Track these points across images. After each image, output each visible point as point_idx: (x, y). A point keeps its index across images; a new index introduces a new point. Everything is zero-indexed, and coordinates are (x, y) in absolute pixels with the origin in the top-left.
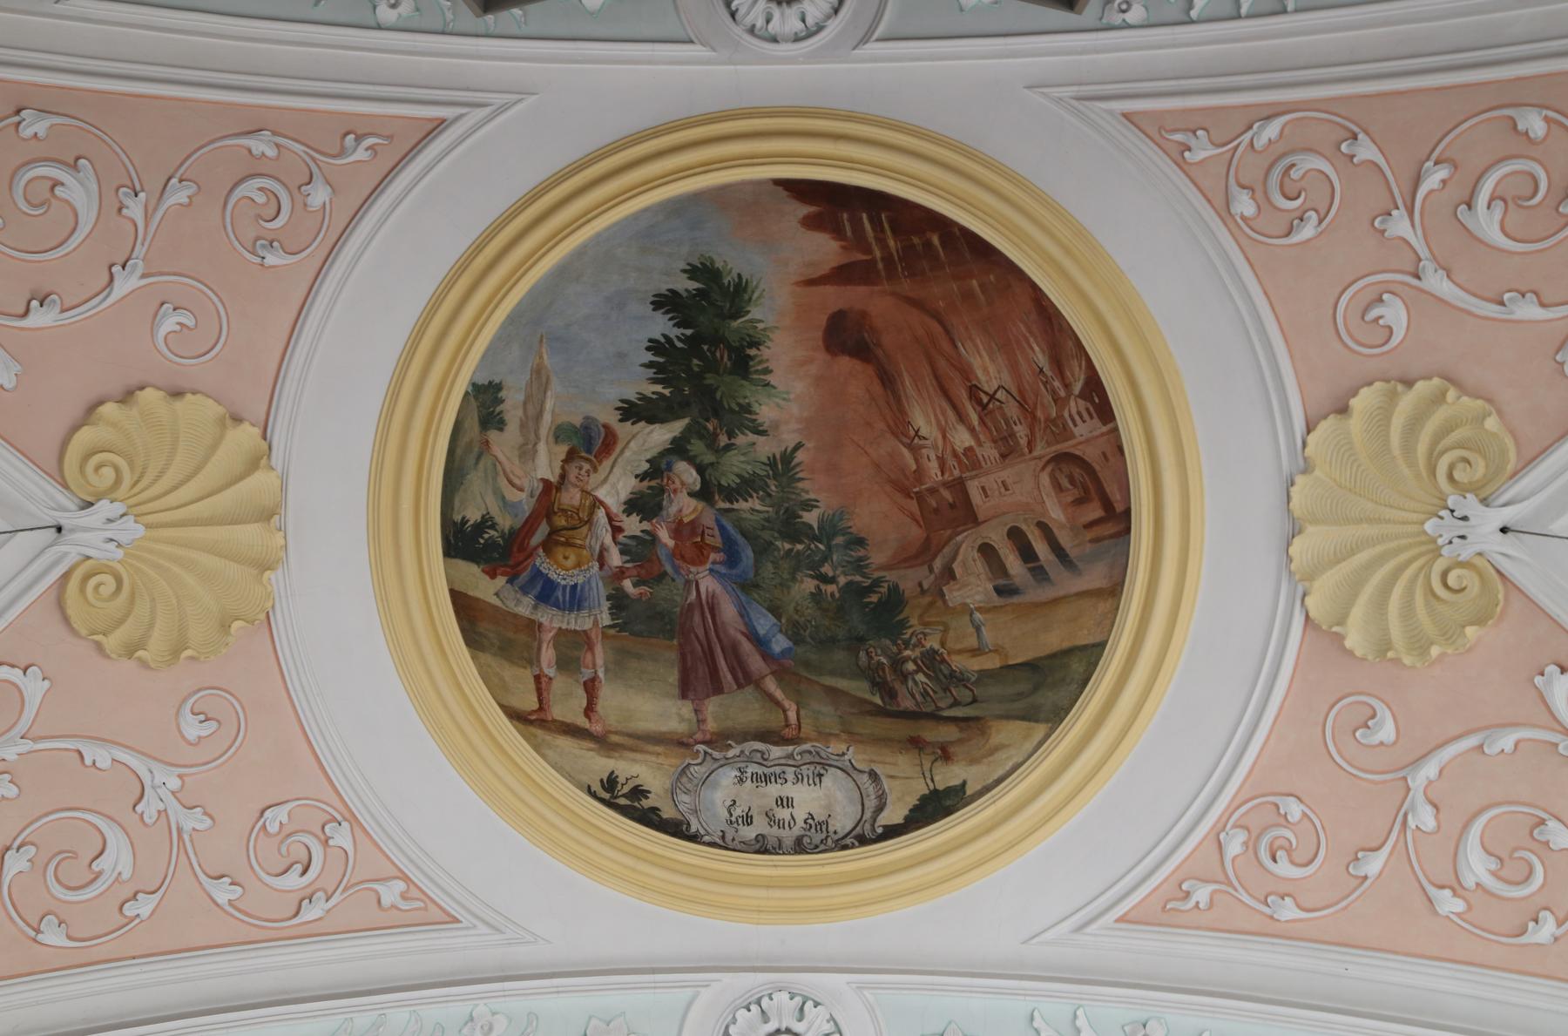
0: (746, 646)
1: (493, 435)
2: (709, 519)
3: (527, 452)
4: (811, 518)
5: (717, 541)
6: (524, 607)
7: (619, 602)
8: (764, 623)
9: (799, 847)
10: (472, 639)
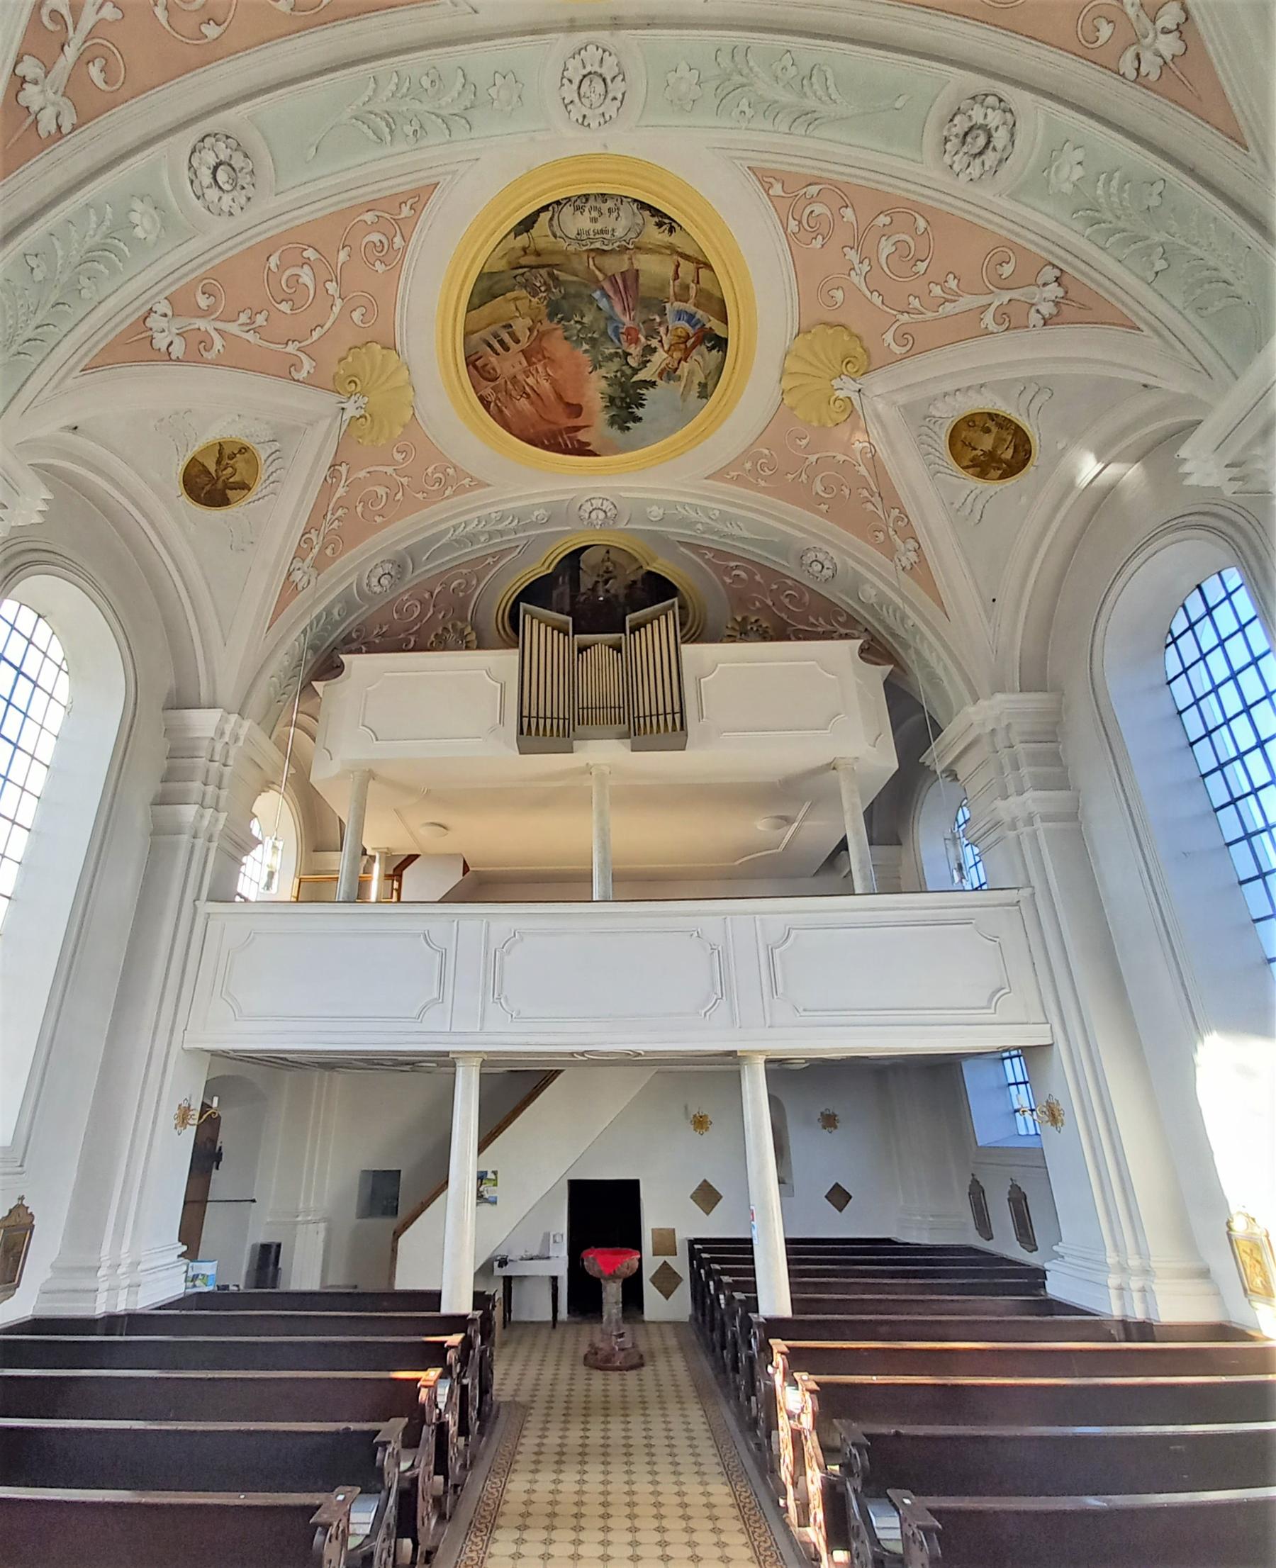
0: (611, 294)
1: (703, 381)
2: (625, 345)
3: (691, 373)
4: (585, 347)
5: (623, 337)
6: (700, 314)
7: (662, 313)
8: (604, 304)
9: (587, 197)
10: (722, 302)
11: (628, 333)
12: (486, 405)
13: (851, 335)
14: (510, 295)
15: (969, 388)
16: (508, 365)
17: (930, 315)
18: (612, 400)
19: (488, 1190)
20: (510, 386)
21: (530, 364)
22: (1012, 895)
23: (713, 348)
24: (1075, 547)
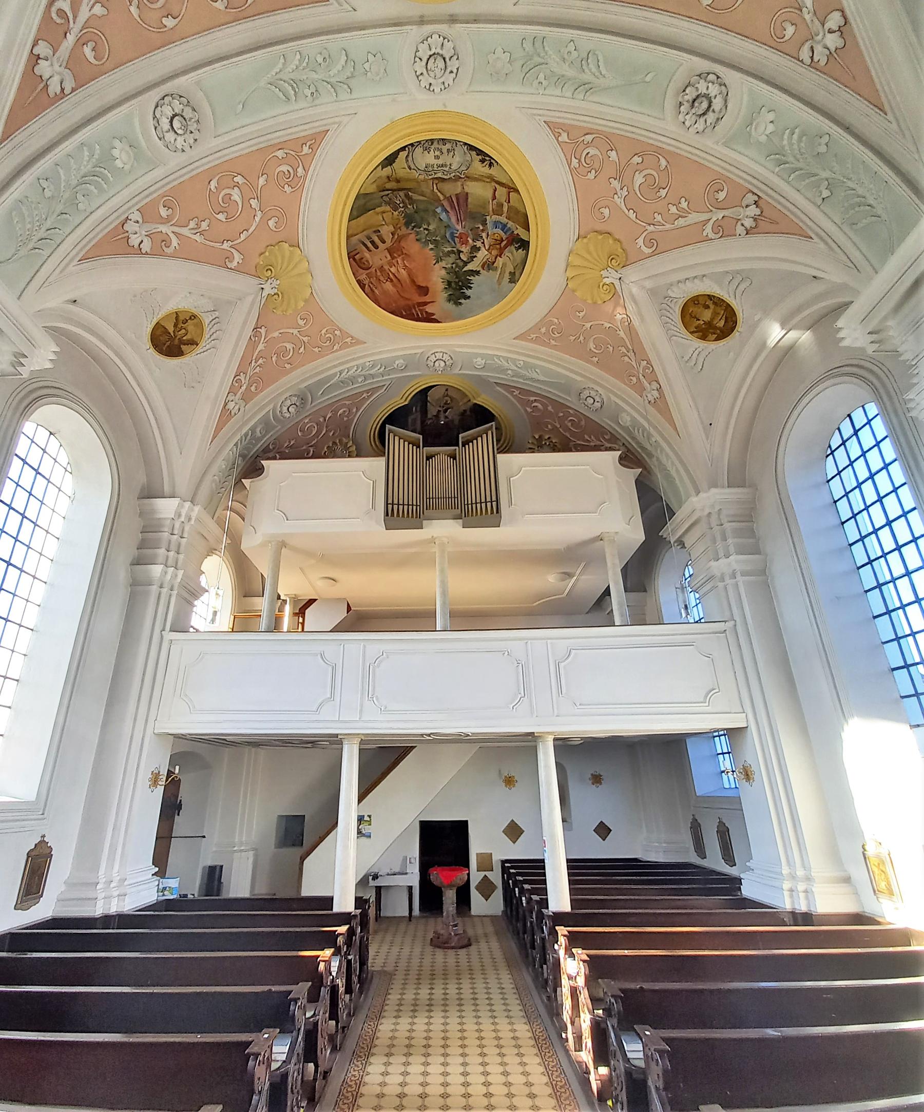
2: (458, 245)
3: (504, 265)
4: (431, 246)
6: (510, 224)
7: (484, 223)
12: (362, 287)
14: (378, 210)
16: (378, 258)
18: (449, 283)
20: (379, 274)
21: (393, 258)
23: (519, 248)
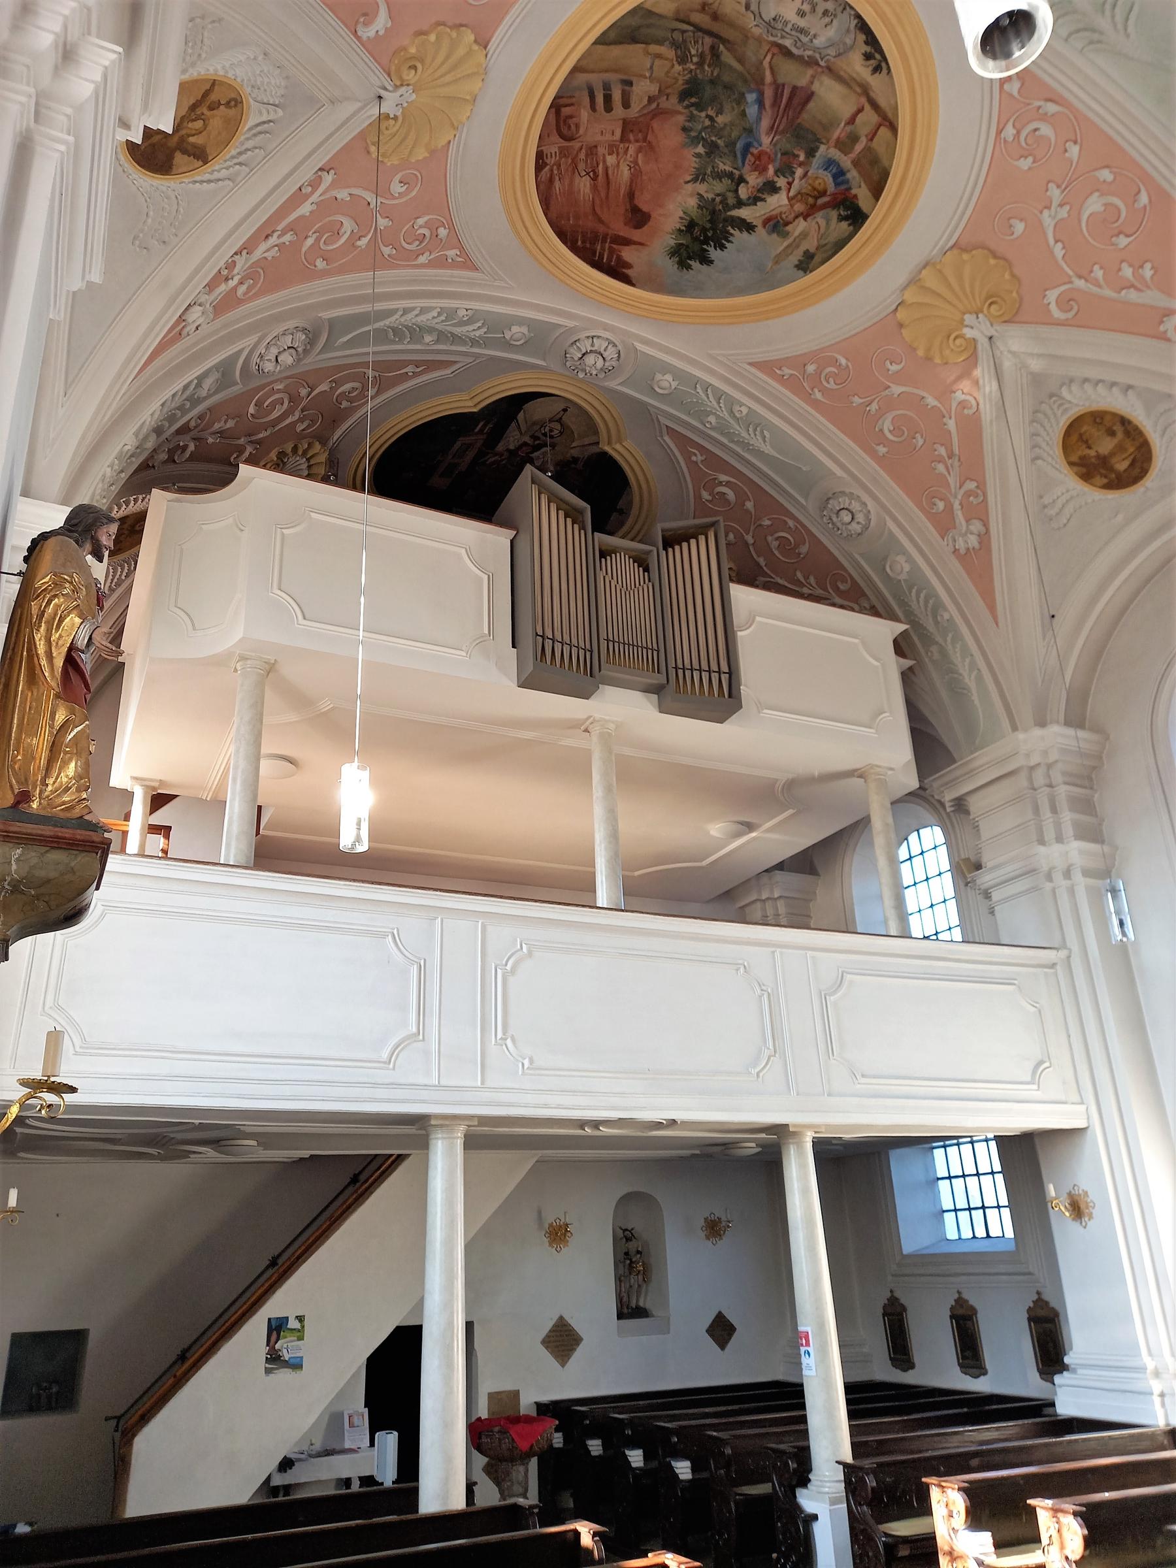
1: (812, 250)
2: (747, 168)
4: (700, 149)
6: (853, 175)
7: (811, 153)
11: (758, 157)
13: (1013, 275)
14: (654, 48)
15: (1113, 384)
16: (597, 129)
17: (1108, 293)
18: (691, 225)
19: (287, 1347)
20: (582, 156)
21: (624, 139)
22: (1050, 955)
23: (846, 218)
24: (1148, 580)
